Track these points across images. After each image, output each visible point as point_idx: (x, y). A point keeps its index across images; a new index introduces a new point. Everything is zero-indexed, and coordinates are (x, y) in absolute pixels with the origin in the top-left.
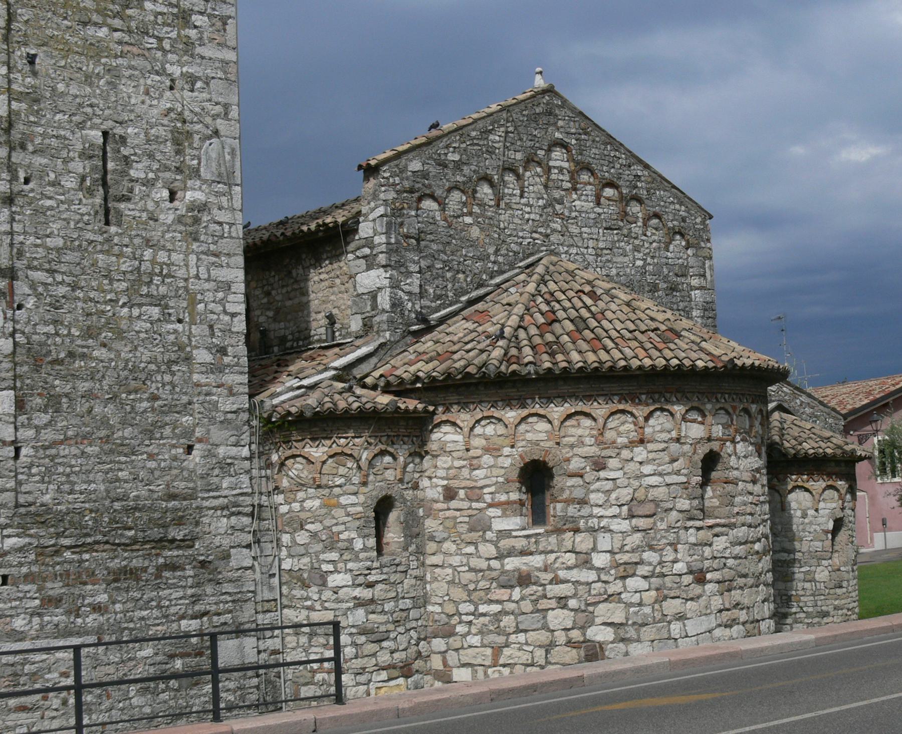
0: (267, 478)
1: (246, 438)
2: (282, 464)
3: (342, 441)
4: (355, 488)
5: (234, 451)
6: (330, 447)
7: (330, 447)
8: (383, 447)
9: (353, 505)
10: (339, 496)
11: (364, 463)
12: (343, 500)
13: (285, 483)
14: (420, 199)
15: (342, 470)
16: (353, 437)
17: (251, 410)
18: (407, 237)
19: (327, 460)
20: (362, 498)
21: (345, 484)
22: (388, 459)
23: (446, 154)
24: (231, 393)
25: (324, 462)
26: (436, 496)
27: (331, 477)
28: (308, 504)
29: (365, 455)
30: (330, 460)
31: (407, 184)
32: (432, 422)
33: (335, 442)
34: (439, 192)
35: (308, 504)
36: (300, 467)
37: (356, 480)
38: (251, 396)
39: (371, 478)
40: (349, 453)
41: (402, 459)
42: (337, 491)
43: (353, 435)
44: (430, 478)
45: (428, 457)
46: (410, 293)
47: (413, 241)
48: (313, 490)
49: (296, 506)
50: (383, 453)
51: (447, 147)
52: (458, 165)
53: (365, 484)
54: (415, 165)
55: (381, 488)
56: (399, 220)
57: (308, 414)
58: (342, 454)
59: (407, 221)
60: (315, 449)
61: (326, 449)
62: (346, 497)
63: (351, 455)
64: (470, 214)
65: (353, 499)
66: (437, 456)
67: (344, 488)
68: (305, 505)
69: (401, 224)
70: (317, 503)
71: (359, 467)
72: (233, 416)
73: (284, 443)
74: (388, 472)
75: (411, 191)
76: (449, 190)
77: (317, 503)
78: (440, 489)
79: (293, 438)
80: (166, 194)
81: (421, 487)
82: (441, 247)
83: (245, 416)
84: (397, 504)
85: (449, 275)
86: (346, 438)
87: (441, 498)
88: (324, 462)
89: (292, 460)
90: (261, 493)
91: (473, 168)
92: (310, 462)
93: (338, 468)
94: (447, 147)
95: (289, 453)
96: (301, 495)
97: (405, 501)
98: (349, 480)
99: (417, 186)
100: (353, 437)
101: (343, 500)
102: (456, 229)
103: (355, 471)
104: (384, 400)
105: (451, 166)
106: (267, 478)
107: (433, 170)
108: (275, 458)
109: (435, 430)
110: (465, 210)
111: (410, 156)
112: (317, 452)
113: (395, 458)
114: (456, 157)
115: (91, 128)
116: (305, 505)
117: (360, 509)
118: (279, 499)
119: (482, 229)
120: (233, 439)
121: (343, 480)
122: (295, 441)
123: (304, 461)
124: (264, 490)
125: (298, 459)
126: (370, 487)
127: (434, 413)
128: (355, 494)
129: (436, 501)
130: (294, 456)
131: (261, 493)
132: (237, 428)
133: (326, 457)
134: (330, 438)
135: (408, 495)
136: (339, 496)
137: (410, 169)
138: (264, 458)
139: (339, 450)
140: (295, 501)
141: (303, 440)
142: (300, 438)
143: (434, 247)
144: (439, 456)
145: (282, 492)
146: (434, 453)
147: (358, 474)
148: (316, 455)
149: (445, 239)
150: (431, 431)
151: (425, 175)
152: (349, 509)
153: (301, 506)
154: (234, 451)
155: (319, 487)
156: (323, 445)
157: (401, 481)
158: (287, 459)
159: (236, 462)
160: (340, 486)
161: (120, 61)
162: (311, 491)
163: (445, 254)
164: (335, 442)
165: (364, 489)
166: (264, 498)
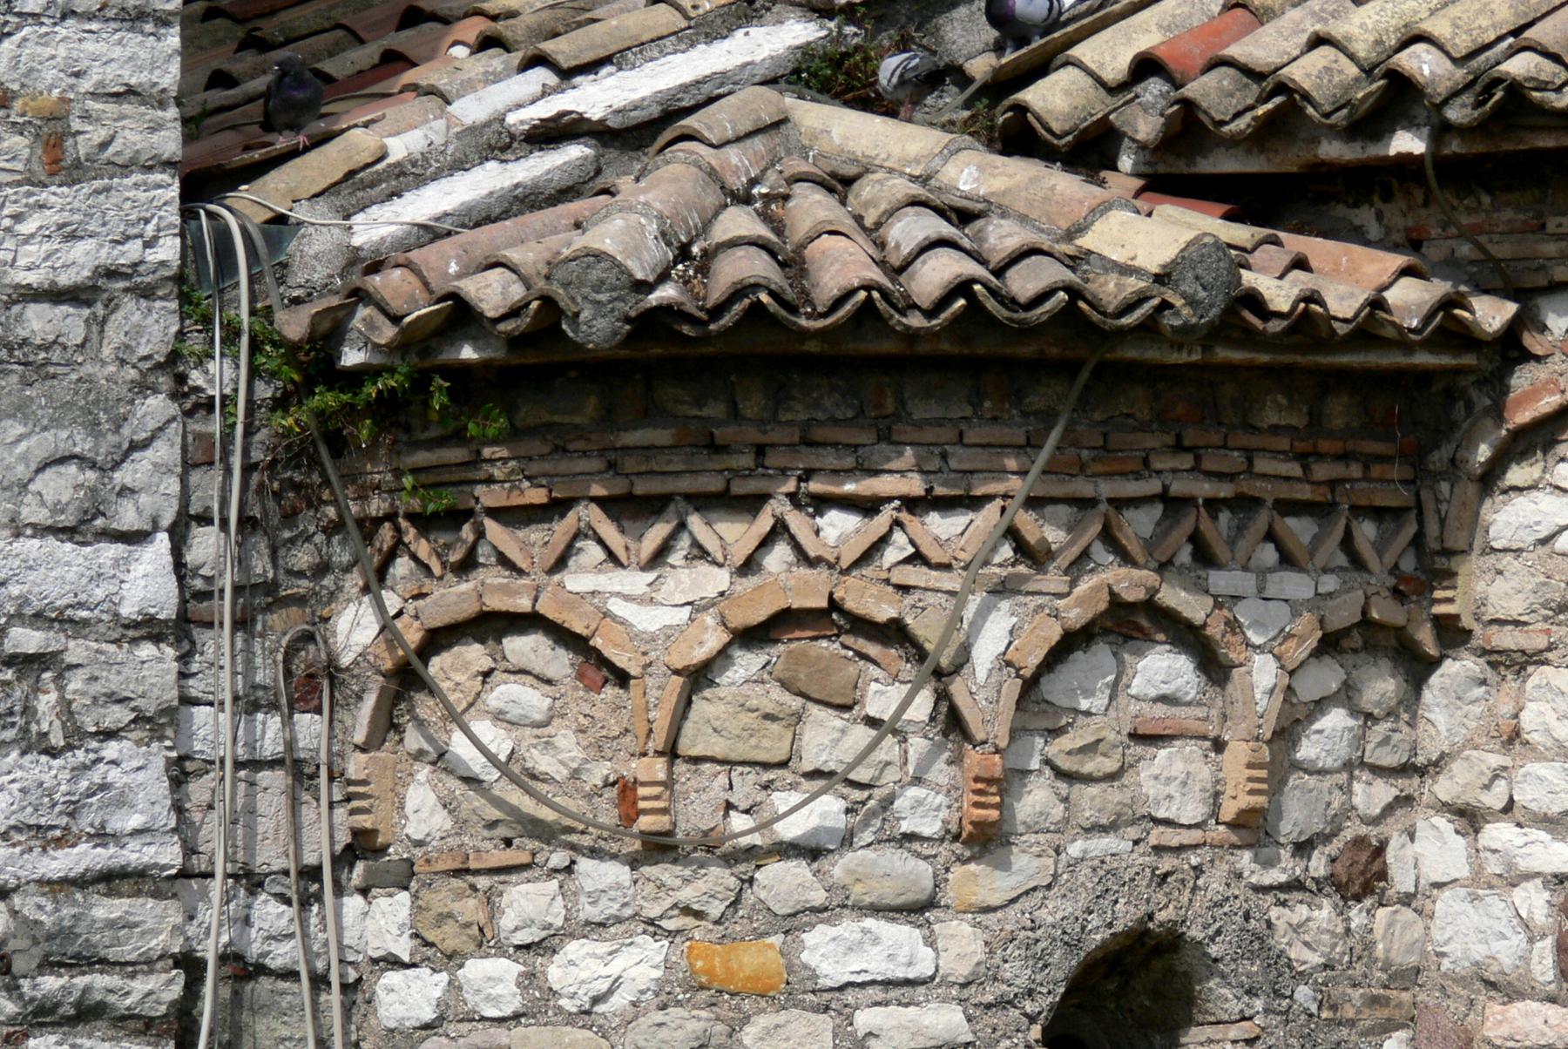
0: (299, 771)
1: (151, 482)
2: (407, 679)
3: (838, 527)
4: (907, 872)
5: (61, 570)
6: (749, 566)
7: (749, 566)
8: (1131, 582)
10: (796, 920)
11: (984, 692)
12: (830, 952)
13: (422, 813)
15: (827, 739)
16: (913, 504)
17: (195, 285)
19: (723, 656)
20: (961, 946)
21: (847, 840)
22: (1162, 669)
24: (58, 159)
25: (699, 677)
26: (1505, 952)
27: (745, 785)
28: (577, 969)
29: (998, 637)
30: (747, 663)
32: (1498, 412)
33: (779, 529)
35: (577, 969)
36: (532, 700)
37: (925, 811)
38: (202, 185)
39: (1037, 799)
40: (883, 610)
41: (1263, 674)
42: (784, 881)
43: (914, 485)
44: (1469, 818)
45: (1458, 668)
48: (616, 872)
49: (493, 980)
50: (1127, 624)
53: (985, 840)
55: (1107, 874)
57: (595, 326)
60: (637, 581)
61: (720, 579)
62: (849, 928)
63: (894, 633)
65: (896, 947)
66: (1519, 663)
67: (840, 867)
68: (555, 973)
70: (640, 963)
71: (952, 723)
72: (69, 322)
73: (425, 523)
77: (640, 963)
78: (1535, 901)
79: (490, 496)
81: (1401, 879)
83: (152, 326)
84: (1222, 996)
86: (867, 507)
87: (1544, 967)
88: (699, 677)
89: (474, 654)
90: (250, 880)
92: (602, 670)
93: (798, 717)
95: (454, 598)
96: (527, 904)
97: (1277, 974)
98: (871, 806)
100: (913, 504)
101: (830, 952)
103: (917, 745)
104: (1142, 239)
106: (299, 771)
108: (355, 629)
109: (1517, 474)
112: (655, 597)
113: (1214, 667)
116: (555, 973)
118: (378, 921)
120: (61, 486)
121: (828, 811)
122: (494, 513)
123: (560, 662)
124: (270, 856)
125: (521, 647)
126: (1026, 865)
127: (1510, 348)
128: (917, 910)
129: (1506, 989)
130: (490, 625)
131: (250, 880)
132: (94, 410)
133: (714, 639)
134: (752, 504)
135: (1310, 929)
136: (796, 920)
138: (281, 625)
139: (810, 590)
140: (485, 941)
141: (557, 508)
142: (537, 496)
144: (1535, 658)
145: (404, 877)
146: (1506, 639)
147: (941, 772)
148: (647, 620)
150: (1489, 480)
152: (865, 1019)
153: (529, 979)
154: (61, 570)
155: (660, 848)
156: (700, 553)
157: (1254, 828)
158: (439, 639)
159: (77, 651)
160: (810, 851)
162: (603, 877)
164: (779, 529)
165: (979, 882)
166: (270, 913)
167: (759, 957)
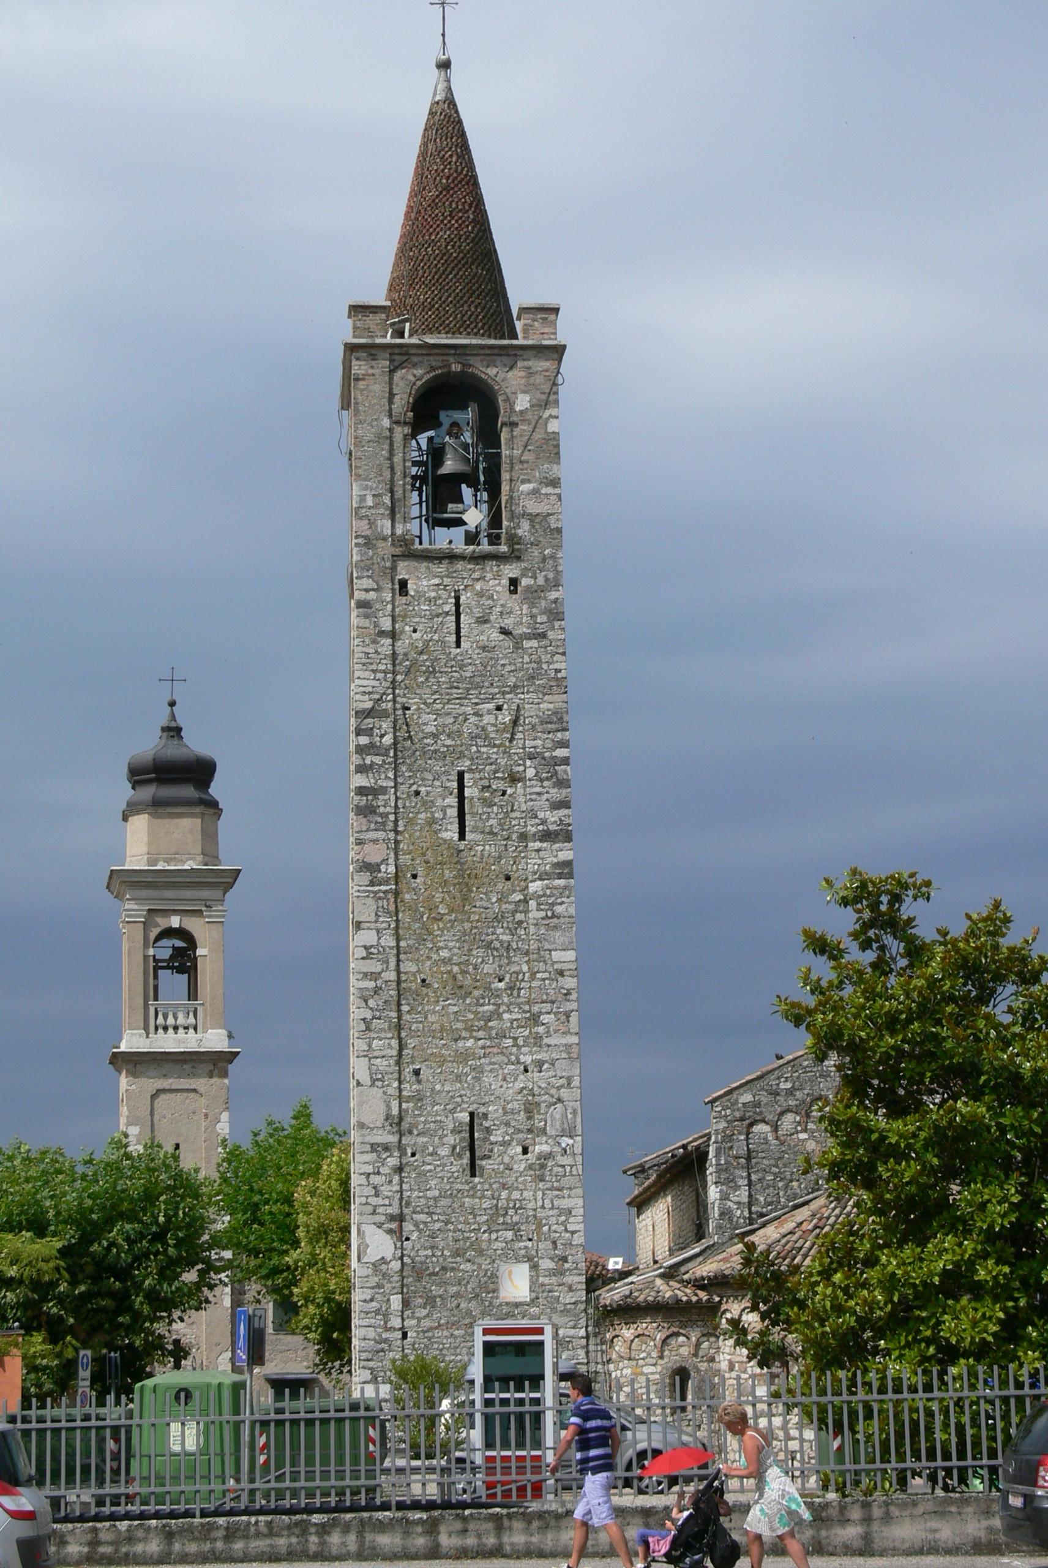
0: (602, 1352)
1: (583, 1322)
2: (612, 1341)
3: (644, 1325)
4: (654, 1361)
5: (572, 1332)
8: (676, 1330)
9: (652, 1373)
12: (646, 1370)
14: (751, 1125)
17: (588, 1301)
18: (737, 1157)
20: (659, 1368)
22: (681, 1339)
23: (778, 1085)
24: (570, 1289)
25: (632, 1341)
29: (659, 1336)
31: (738, 1115)
34: (769, 1117)
38: (588, 1291)
39: (666, 1353)
41: (694, 1339)
42: (641, 1362)
46: (738, 1203)
47: (743, 1160)
50: (677, 1334)
51: (778, 1078)
52: (790, 1092)
53: (661, 1357)
54: (747, 1098)
55: (676, 1361)
56: (729, 1144)
58: (643, 1335)
59: (736, 1144)
64: (805, 1130)
65: (652, 1369)
69: (731, 1148)
72: (573, 1307)
74: (682, 1349)
75: (742, 1119)
76: (782, 1114)
80: (519, 1149)
82: (772, 1162)
83: (583, 1306)
85: (780, 1184)
90: (597, 1363)
91: (806, 1092)
94: (778, 1078)
97: (698, 1371)
98: (649, 1354)
99: (748, 1114)
101: (646, 1370)
102: (789, 1145)
105: (783, 1094)
106: (602, 1352)
107: (764, 1099)
110: (799, 1128)
111: (741, 1090)
112: (628, 1333)
113: (688, 1338)
114: (789, 1085)
115: (461, 1112)
117: (658, 1376)
118: (611, 1367)
119: (817, 1142)
120: (572, 1323)
124: (599, 1360)
126: (666, 1360)
127: (720, 1302)
128: (654, 1365)
131: (597, 1363)
132: (575, 1315)
135: (703, 1366)
137: (741, 1101)
138: (600, 1337)
143: (765, 1162)
149: (777, 1155)
151: (757, 1104)
154: (572, 1332)
157: (696, 1355)
160: (643, 1359)
161: (483, 1060)
163: (777, 1167)
165: (660, 1362)
166: (600, 1366)
167: (639, 1370)
